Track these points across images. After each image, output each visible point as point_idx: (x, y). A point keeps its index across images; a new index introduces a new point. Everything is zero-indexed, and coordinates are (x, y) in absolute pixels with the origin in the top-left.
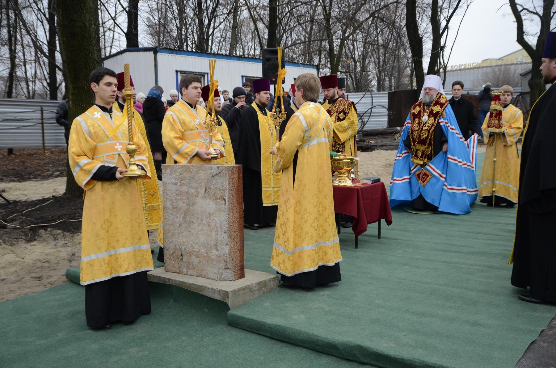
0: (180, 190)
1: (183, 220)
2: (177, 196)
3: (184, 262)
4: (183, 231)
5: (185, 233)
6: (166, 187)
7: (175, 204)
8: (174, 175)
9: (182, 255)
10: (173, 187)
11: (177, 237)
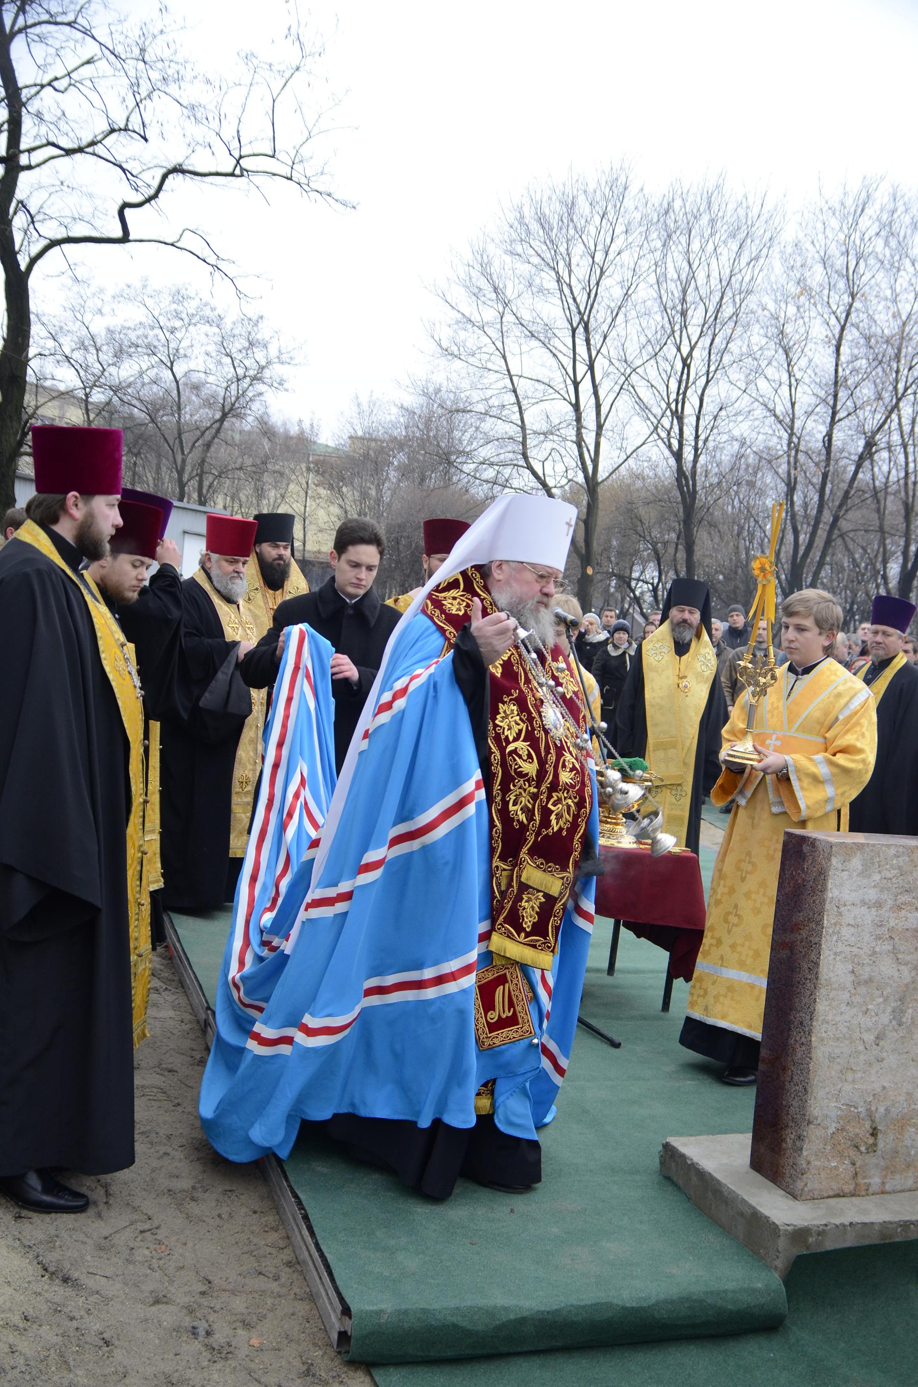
0: (892, 923)
1: (894, 1018)
2: (879, 942)
3: (879, 1153)
4: (885, 1054)
5: (892, 1060)
6: (840, 914)
7: (867, 969)
8: (877, 877)
9: (874, 1133)
10: (868, 916)
11: (859, 1075)
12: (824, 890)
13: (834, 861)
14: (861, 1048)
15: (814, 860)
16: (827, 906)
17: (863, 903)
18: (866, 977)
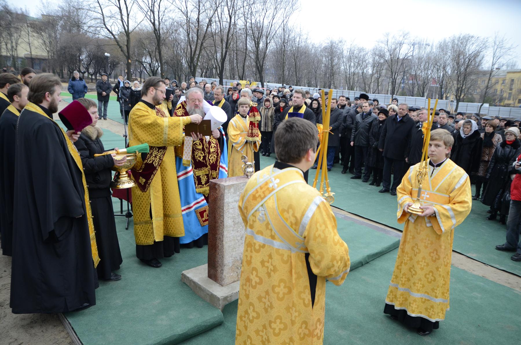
6: (229, 206)
8: (238, 193)
11: (237, 249)
12: (223, 200)
13: (226, 191)
14: (237, 242)
15: (220, 190)
16: (225, 204)
17: (235, 201)
18: (237, 222)
